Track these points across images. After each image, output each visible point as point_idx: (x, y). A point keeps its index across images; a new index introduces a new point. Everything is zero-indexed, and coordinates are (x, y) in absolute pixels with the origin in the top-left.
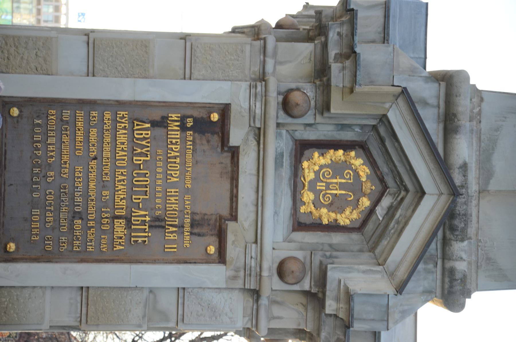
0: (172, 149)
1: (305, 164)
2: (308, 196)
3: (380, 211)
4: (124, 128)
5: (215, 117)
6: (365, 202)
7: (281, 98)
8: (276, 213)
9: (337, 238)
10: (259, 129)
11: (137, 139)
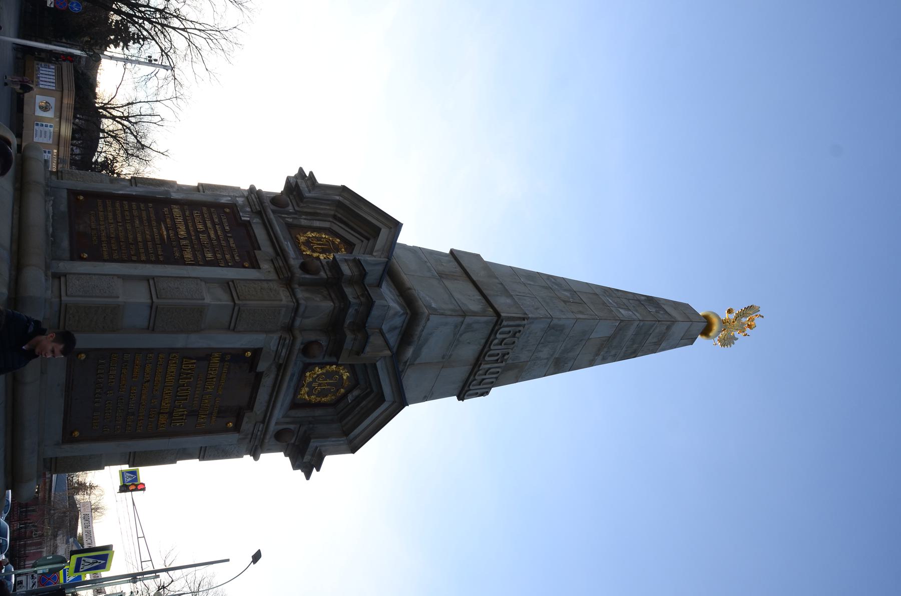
0: (211, 374)
1: (308, 374)
2: (305, 389)
3: (350, 398)
5: (249, 354)
7: (302, 347)
8: (282, 406)
9: (318, 412)
10: (281, 365)
11: (184, 369)
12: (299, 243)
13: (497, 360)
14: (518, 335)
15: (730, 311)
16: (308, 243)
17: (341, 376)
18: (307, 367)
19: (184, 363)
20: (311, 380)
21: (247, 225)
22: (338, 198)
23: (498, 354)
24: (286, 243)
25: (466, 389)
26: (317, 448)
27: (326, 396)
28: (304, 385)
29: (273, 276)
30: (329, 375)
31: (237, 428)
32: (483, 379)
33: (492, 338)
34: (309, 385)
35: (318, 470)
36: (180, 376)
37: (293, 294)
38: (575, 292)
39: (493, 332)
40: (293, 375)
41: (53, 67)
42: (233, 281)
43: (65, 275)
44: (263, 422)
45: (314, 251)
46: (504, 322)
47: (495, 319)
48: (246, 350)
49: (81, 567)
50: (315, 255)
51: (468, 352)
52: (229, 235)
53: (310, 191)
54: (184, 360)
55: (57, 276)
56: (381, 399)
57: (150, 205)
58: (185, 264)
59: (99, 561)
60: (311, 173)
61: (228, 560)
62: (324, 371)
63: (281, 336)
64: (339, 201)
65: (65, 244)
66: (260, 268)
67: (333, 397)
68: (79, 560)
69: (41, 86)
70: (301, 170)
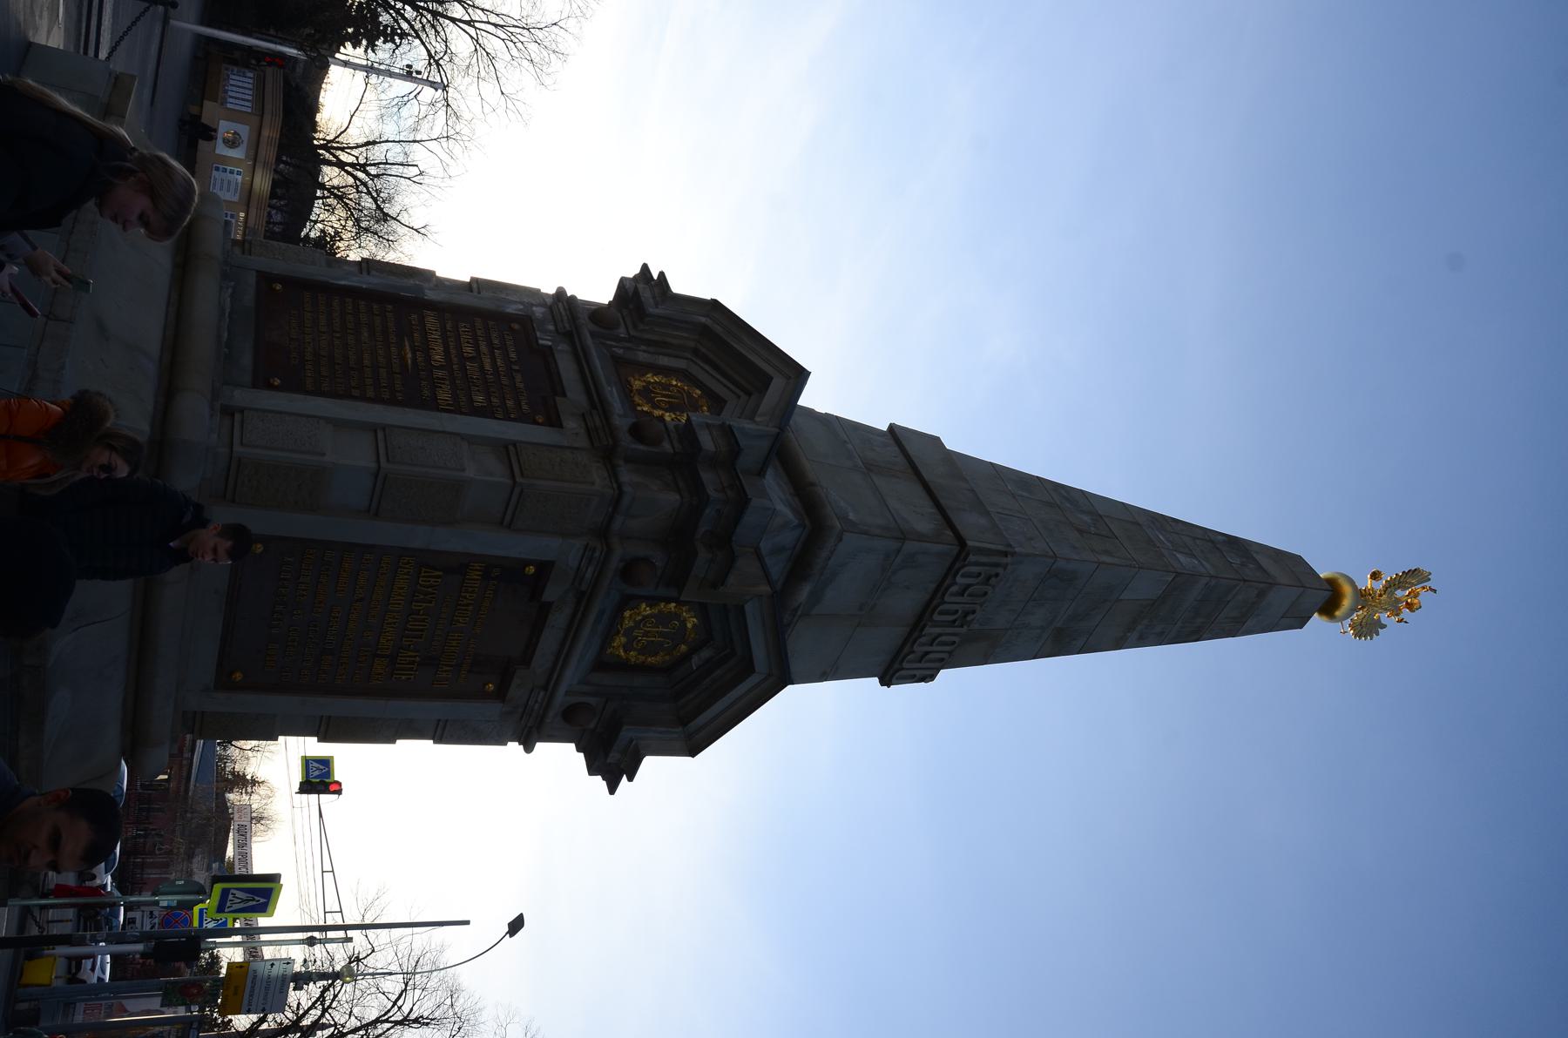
0: (465, 598)
1: (627, 614)
4: (408, 574)
5: (531, 570)
6: (683, 648)
11: (421, 585)
12: (631, 391)
13: (954, 621)
14: (993, 580)
15: (1375, 576)
16: (647, 392)
17: (684, 622)
18: (627, 601)
19: (423, 574)
20: (632, 624)
21: (547, 354)
22: (703, 320)
23: (957, 611)
24: (609, 389)
25: (896, 666)
26: (631, 740)
27: (656, 654)
28: (618, 632)
29: (583, 442)
31: (501, 694)
32: (927, 653)
33: (948, 582)
34: (628, 632)
35: (630, 779)
36: (414, 596)
37: (613, 474)
38: (1101, 516)
39: (951, 571)
41: (251, 75)
42: (514, 445)
43: (242, 411)
44: (545, 688)
45: (656, 406)
46: (971, 555)
47: (956, 549)
48: (527, 563)
49: (228, 904)
50: (657, 413)
51: (905, 602)
52: (516, 368)
53: (657, 305)
54: (424, 569)
55: (229, 412)
56: (748, 668)
57: (390, 307)
58: (438, 410)
59: (257, 898)
60: (662, 274)
61: (467, 923)
62: (655, 611)
63: (588, 544)
64: (705, 326)
65: (247, 359)
66: (561, 426)
67: (667, 658)
68: (225, 893)
69: (229, 106)
70: (645, 268)
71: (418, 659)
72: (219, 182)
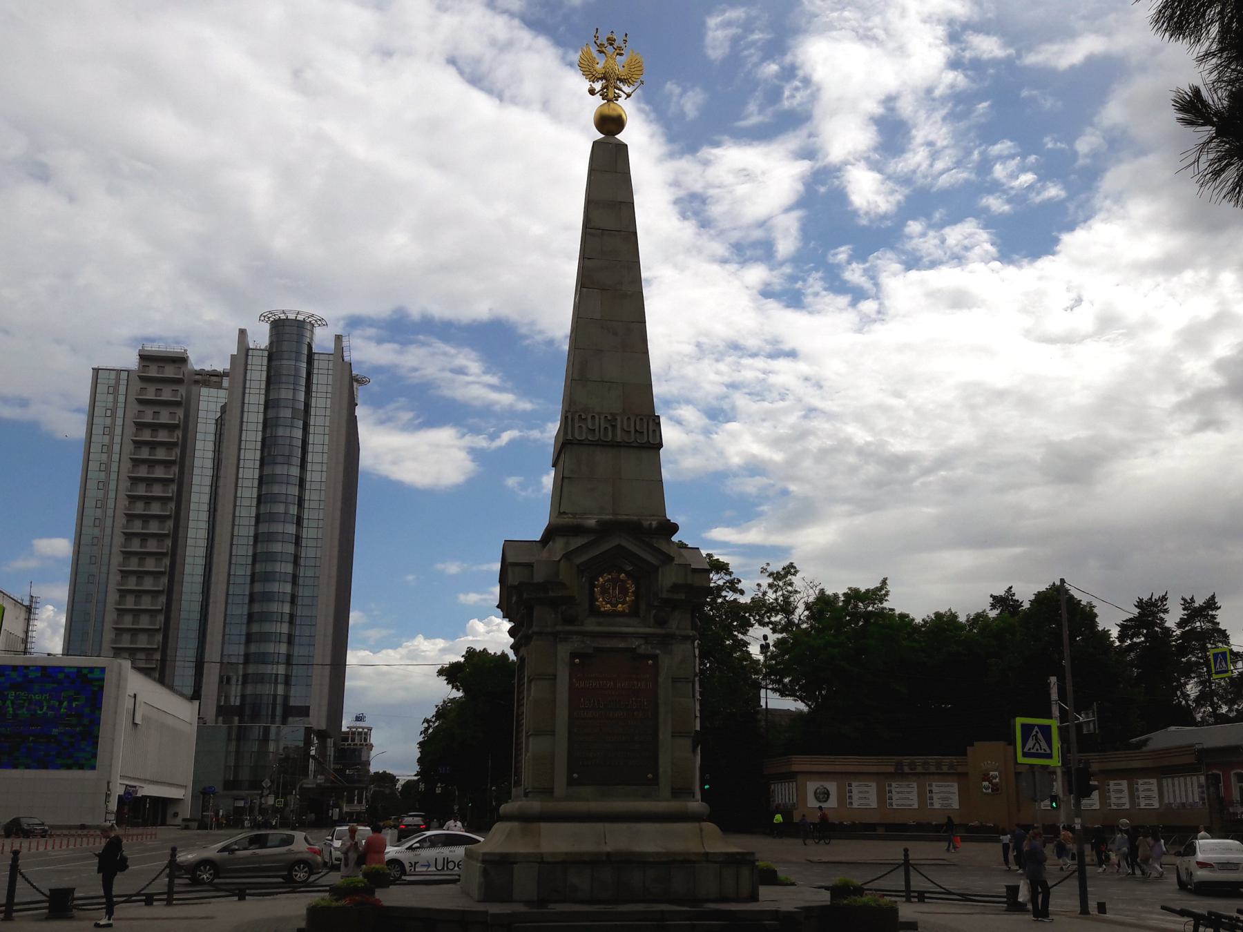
1: (602, 609)
17: (606, 581)
18: (594, 611)
30: (604, 591)
39: (580, 443)
40: (599, 624)
41: (772, 787)
49: (1043, 751)
59: (1034, 733)
69: (795, 801)
71: (634, 699)
72: (863, 801)
